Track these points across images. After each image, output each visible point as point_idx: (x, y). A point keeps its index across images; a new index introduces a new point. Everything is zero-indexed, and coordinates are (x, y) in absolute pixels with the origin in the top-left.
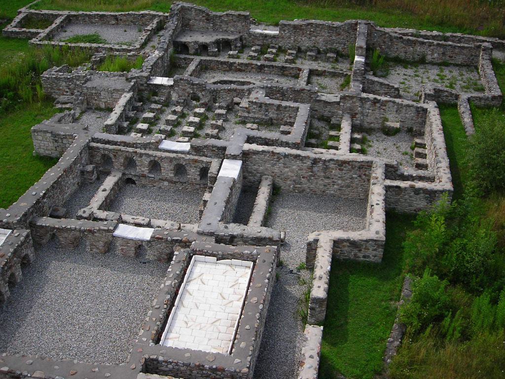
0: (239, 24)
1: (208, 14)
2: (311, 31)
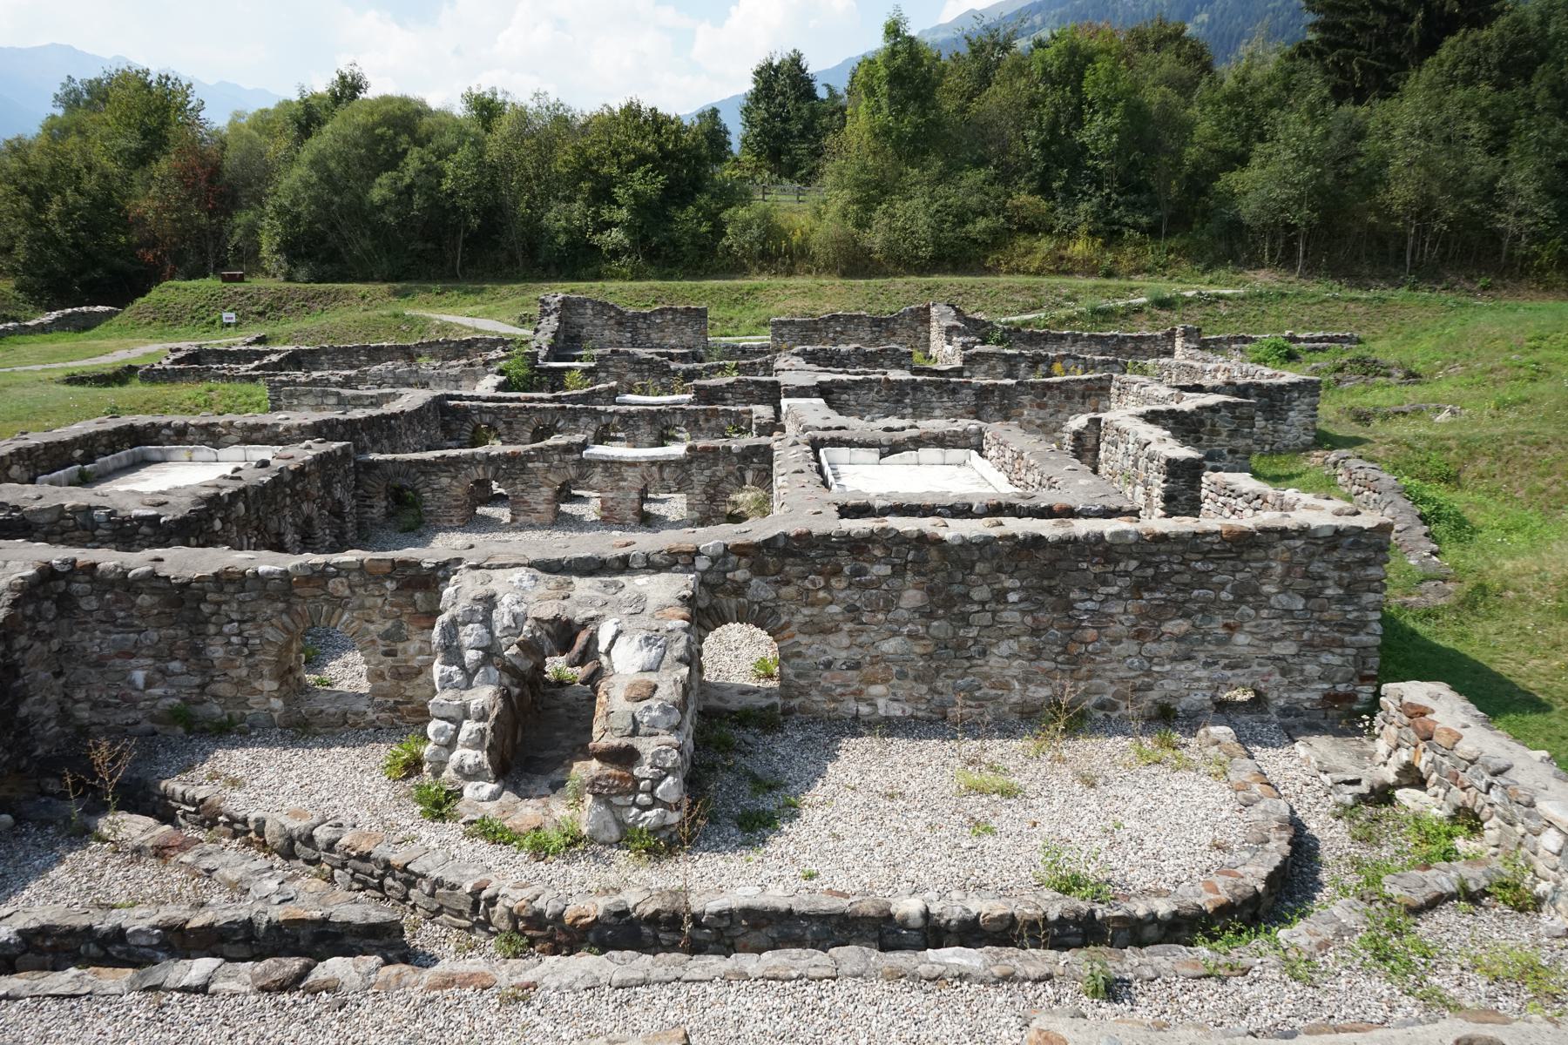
0: (688, 331)
1: (621, 313)
2: (836, 332)
